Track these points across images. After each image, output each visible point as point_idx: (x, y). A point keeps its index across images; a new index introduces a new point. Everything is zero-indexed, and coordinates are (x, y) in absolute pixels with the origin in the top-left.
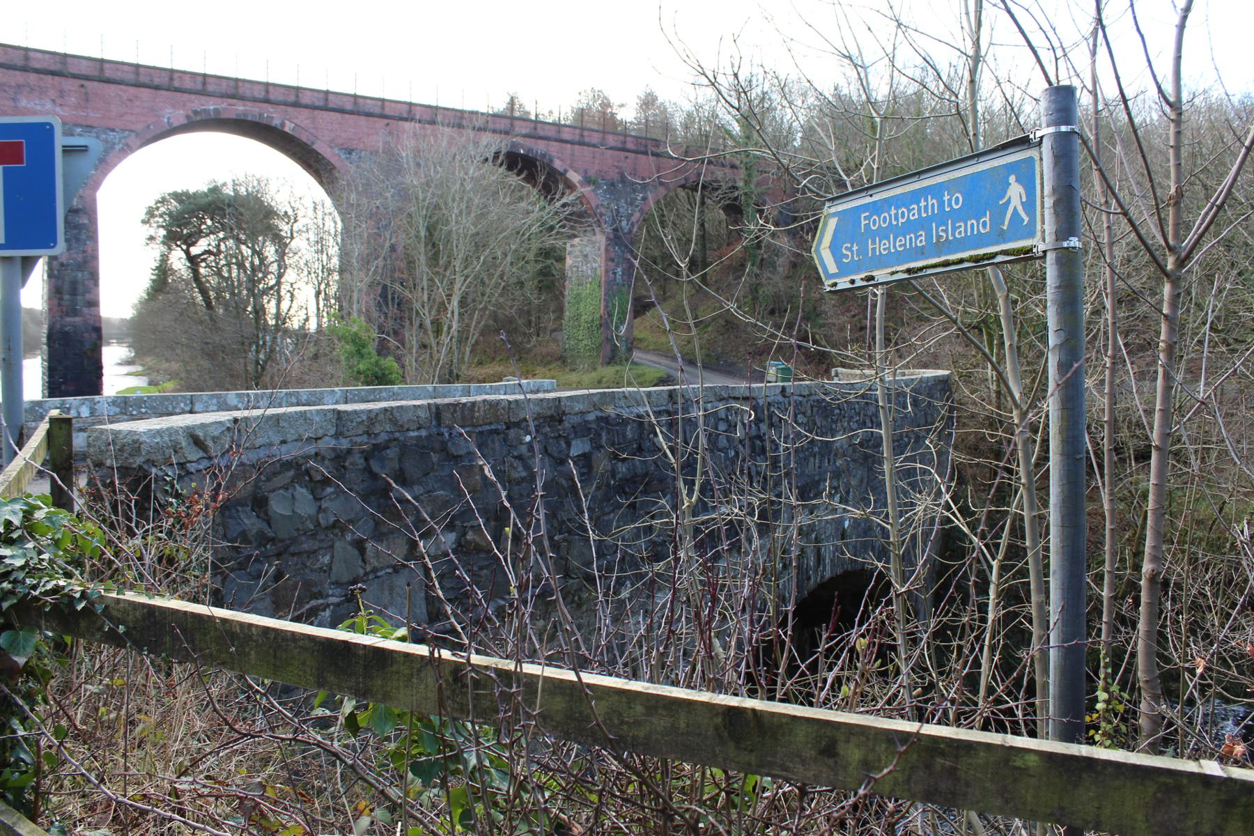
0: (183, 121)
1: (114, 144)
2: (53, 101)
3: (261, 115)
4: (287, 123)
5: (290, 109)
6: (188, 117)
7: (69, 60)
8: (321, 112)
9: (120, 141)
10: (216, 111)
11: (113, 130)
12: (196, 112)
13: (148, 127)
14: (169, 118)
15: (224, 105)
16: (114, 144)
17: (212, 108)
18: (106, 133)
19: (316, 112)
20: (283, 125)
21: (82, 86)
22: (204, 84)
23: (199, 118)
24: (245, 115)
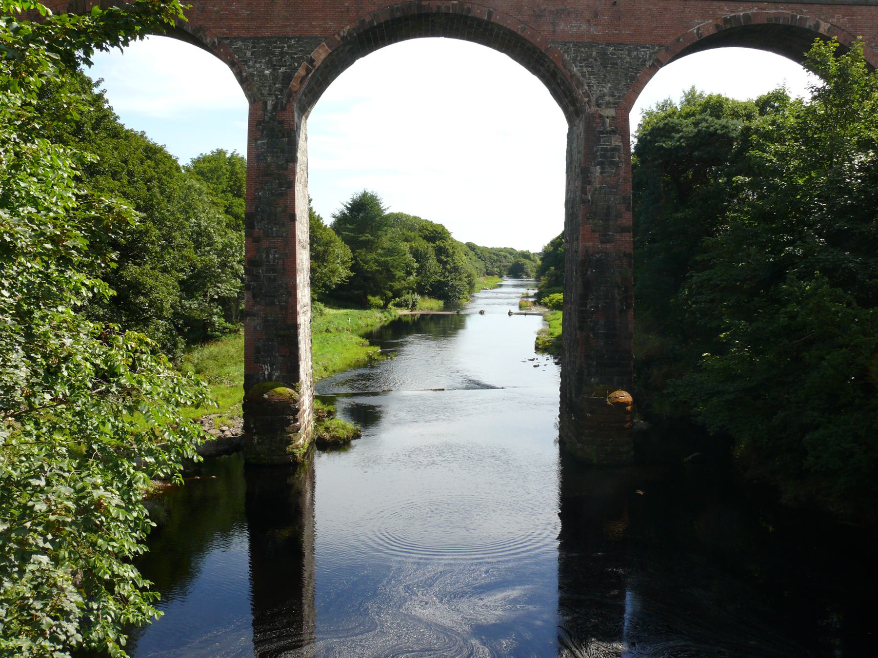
0: (712, 31)
1: (645, 61)
2: (588, 21)
3: (794, 17)
4: (822, 24)
5: (825, 8)
6: (717, 26)
8: (860, 8)
9: (650, 56)
10: (746, 16)
12: (726, 21)
13: (678, 40)
14: (698, 29)
15: (754, 11)
17: (742, 14)
18: (637, 50)
19: (855, 9)
20: (817, 26)
23: (728, 26)
24: (776, 19)
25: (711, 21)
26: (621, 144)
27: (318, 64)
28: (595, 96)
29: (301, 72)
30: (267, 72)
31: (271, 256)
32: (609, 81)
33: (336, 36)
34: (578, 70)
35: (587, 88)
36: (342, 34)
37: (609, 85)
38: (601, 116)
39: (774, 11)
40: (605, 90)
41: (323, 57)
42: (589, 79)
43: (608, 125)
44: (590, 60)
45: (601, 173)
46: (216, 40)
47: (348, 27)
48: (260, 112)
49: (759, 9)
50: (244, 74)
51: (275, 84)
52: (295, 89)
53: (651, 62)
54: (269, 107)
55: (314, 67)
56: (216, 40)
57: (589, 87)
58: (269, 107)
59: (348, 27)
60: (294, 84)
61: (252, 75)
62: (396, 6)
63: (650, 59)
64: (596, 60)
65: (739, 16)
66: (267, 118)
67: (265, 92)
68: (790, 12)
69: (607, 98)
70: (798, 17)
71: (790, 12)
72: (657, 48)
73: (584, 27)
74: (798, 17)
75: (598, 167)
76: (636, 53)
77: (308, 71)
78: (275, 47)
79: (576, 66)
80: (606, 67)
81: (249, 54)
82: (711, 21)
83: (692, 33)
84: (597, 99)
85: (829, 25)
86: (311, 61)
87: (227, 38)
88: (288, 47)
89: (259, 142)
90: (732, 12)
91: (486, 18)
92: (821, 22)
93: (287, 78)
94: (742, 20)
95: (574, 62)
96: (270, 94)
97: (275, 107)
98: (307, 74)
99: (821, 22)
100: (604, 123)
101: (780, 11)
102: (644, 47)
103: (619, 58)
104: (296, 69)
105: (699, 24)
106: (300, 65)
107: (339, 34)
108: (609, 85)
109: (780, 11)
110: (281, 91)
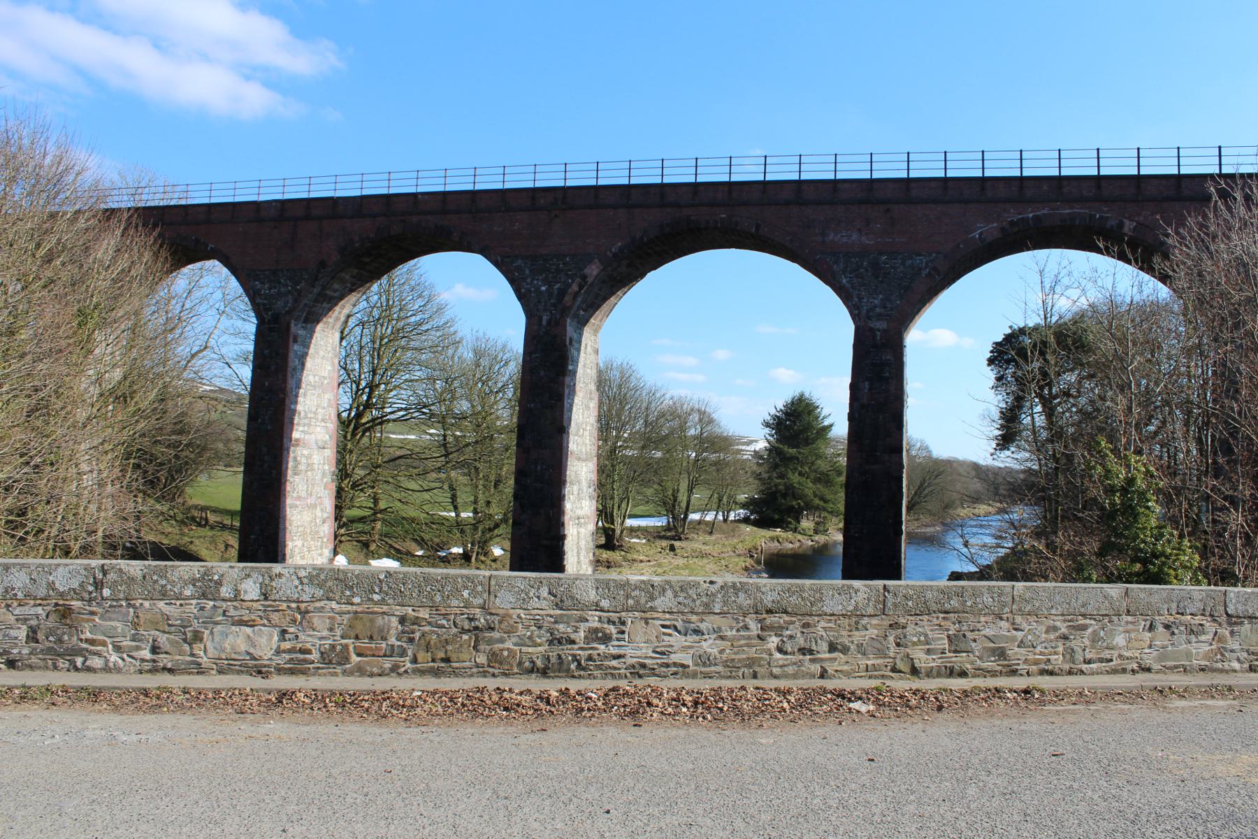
1: (920, 269)
2: (860, 231)
3: (1092, 217)
4: (1127, 222)
6: (1003, 229)
7: (839, 185)
9: (927, 264)
11: (920, 255)
12: (1012, 223)
13: (958, 246)
14: (981, 234)
15: (1045, 211)
16: (920, 269)
17: (1031, 215)
20: (1121, 225)
21: (888, 210)
22: (1021, 188)
23: (1016, 229)
25: (995, 225)
26: (892, 358)
27: (590, 280)
28: (865, 308)
29: (575, 287)
30: (543, 288)
31: (539, 468)
32: (880, 293)
33: (608, 253)
34: (848, 282)
35: (856, 299)
36: (613, 250)
37: (881, 296)
38: (871, 330)
39: (1069, 211)
40: (876, 302)
41: (595, 273)
42: (859, 290)
43: (878, 338)
44: (862, 270)
45: (870, 390)
46: (499, 258)
47: (620, 244)
48: (536, 327)
49: (1051, 210)
50: (523, 290)
51: (550, 299)
52: (568, 305)
53: (928, 270)
54: (544, 323)
55: (586, 283)
56: (499, 258)
57: (860, 299)
58: (544, 323)
59: (620, 244)
60: (567, 298)
61: (530, 291)
62: (665, 222)
63: (925, 268)
64: (867, 270)
65: (1028, 217)
66: (541, 333)
67: (541, 307)
68: (1087, 211)
69: (878, 310)
70: (1098, 216)
71: (1087, 211)
72: (934, 255)
73: (855, 236)
74: (1098, 216)
75: (867, 383)
76: (910, 262)
77: (581, 287)
78: (551, 265)
79: (846, 278)
80: (877, 277)
81: (527, 272)
82: (995, 225)
83: (974, 237)
84: (868, 311)
85: (1135, 224)
86: (584, 277)
87: (509, 257)
88: (563, 264)
89: (534, 356)
90: (1020, 214)
91: (753, 230)
92: (1125, 221)
93: (562, 293)
94: (1031, 222)
95: (844, 272)
96: (545, 310)
97: (549, 322)
98: (580, 290)
99: (1125, 221)
100: (874, 336)
101: (1075, 210)
102: (920, 255)
103: (892, 267)
104: (570, 286)
105: (981, 228)
106: (573, 281)
107: (611, 251)
108: (881, 296)
109: (1075, 210)
110: (554, 305)
